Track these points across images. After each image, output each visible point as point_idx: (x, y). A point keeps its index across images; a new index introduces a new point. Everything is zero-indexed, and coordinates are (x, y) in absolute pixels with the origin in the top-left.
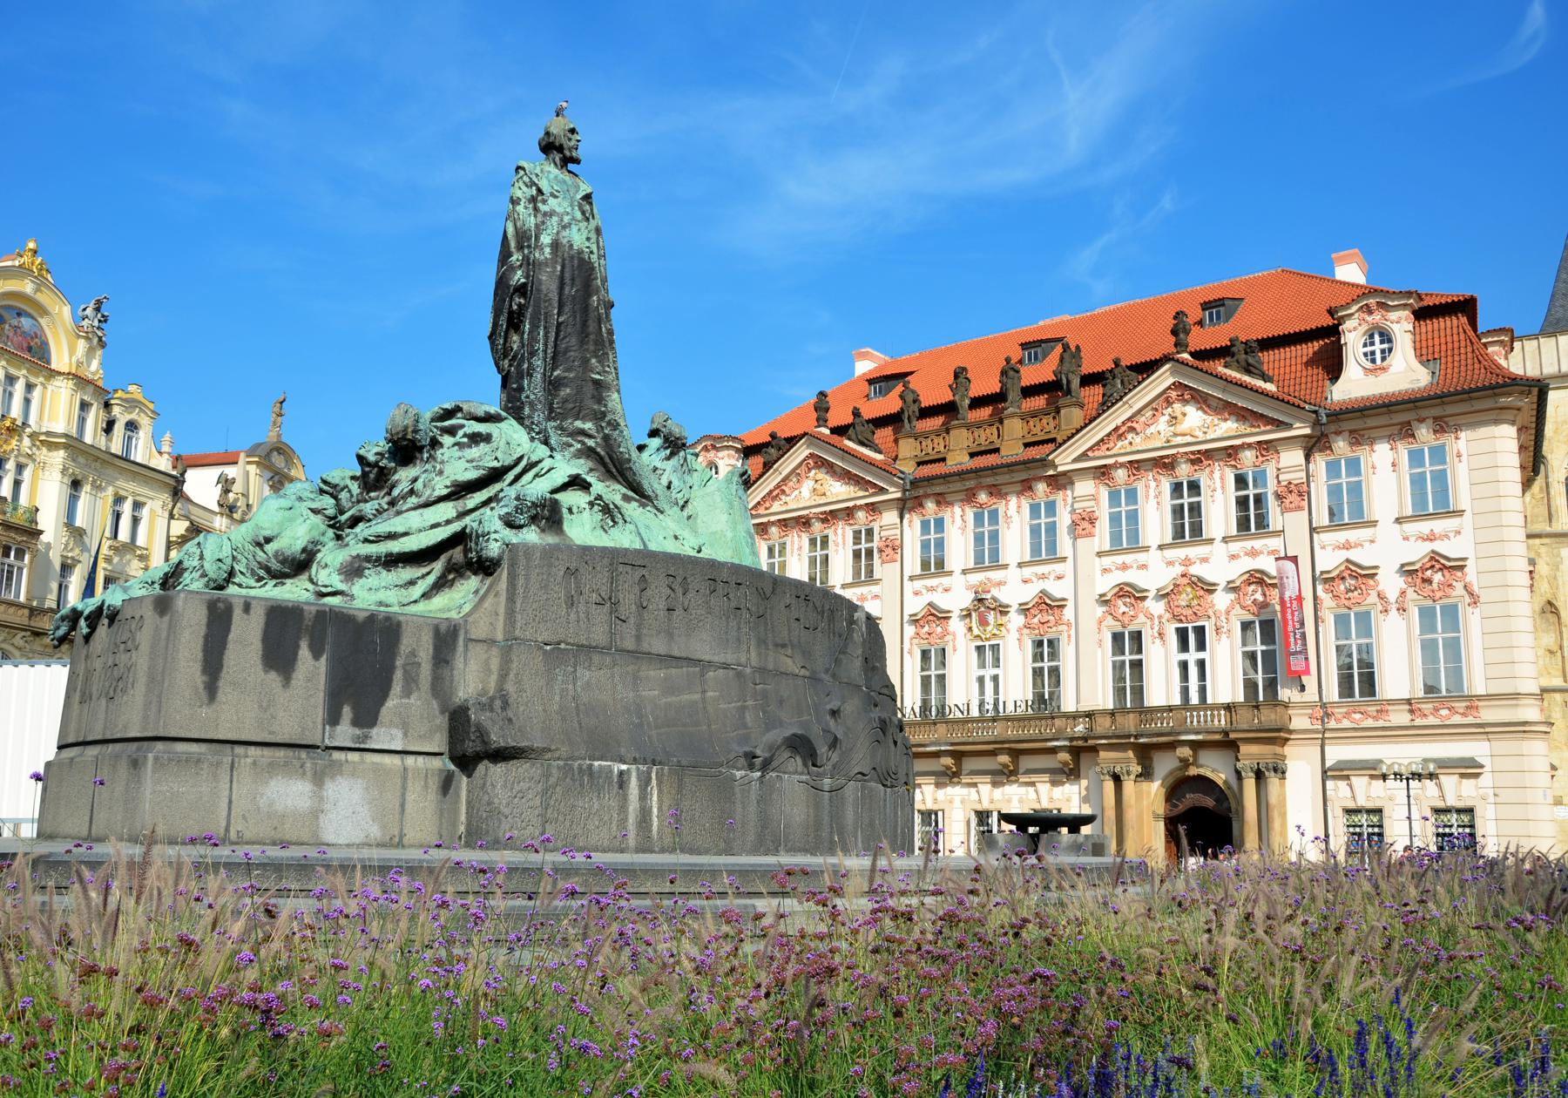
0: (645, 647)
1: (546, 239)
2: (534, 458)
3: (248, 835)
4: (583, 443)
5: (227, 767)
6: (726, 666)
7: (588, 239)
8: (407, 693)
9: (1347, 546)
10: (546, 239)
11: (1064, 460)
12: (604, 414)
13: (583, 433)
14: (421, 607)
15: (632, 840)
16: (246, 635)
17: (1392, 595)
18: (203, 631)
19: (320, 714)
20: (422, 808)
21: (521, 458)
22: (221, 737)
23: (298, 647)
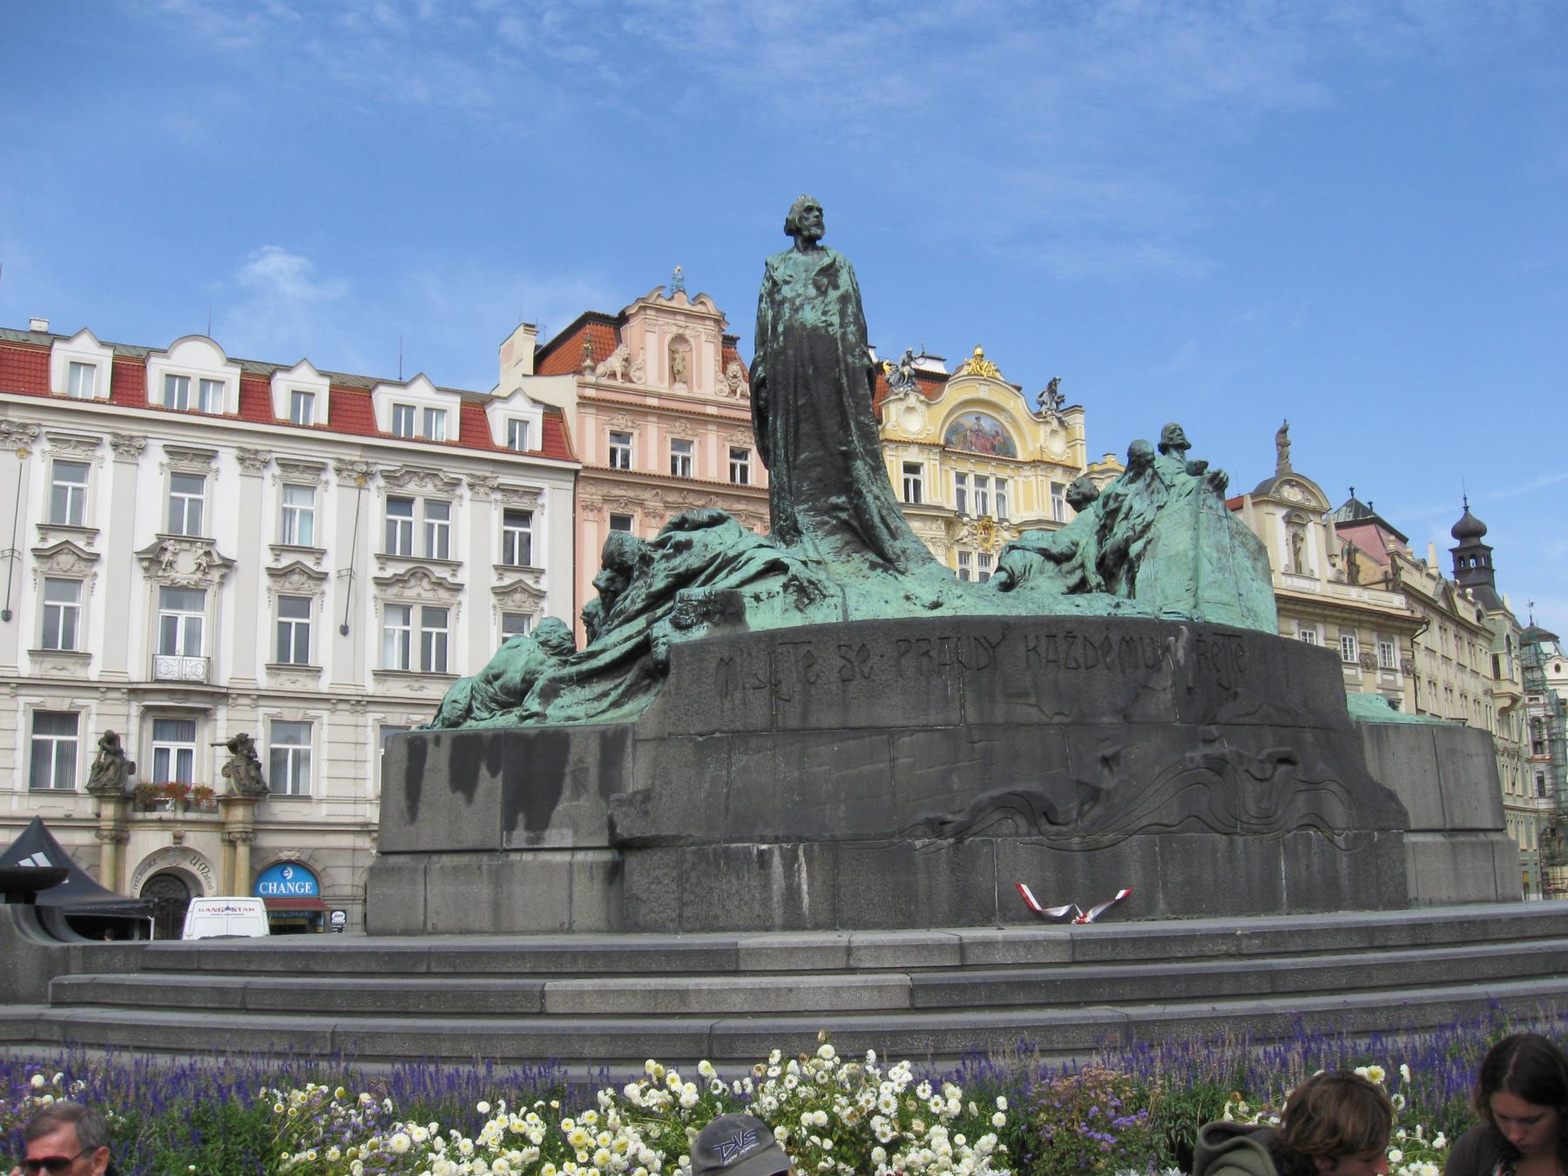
0: (812, 722)
1: (780, 329)
2: (731, 553)
3: (441, 926)
4: (837, 518)
5: (421, 872)
6: (927, 729)
7: (825, 313)
8: (576, 795)
10: (780, 329)
12: (851, 484)
13: (837, 508)
14: (609, 715)
15: (778, 919)
18: (404, 764)
19: (498, 822)
20: (589, 898)
21: (717, 556)
22: (421, 848)
23: (477, 769)
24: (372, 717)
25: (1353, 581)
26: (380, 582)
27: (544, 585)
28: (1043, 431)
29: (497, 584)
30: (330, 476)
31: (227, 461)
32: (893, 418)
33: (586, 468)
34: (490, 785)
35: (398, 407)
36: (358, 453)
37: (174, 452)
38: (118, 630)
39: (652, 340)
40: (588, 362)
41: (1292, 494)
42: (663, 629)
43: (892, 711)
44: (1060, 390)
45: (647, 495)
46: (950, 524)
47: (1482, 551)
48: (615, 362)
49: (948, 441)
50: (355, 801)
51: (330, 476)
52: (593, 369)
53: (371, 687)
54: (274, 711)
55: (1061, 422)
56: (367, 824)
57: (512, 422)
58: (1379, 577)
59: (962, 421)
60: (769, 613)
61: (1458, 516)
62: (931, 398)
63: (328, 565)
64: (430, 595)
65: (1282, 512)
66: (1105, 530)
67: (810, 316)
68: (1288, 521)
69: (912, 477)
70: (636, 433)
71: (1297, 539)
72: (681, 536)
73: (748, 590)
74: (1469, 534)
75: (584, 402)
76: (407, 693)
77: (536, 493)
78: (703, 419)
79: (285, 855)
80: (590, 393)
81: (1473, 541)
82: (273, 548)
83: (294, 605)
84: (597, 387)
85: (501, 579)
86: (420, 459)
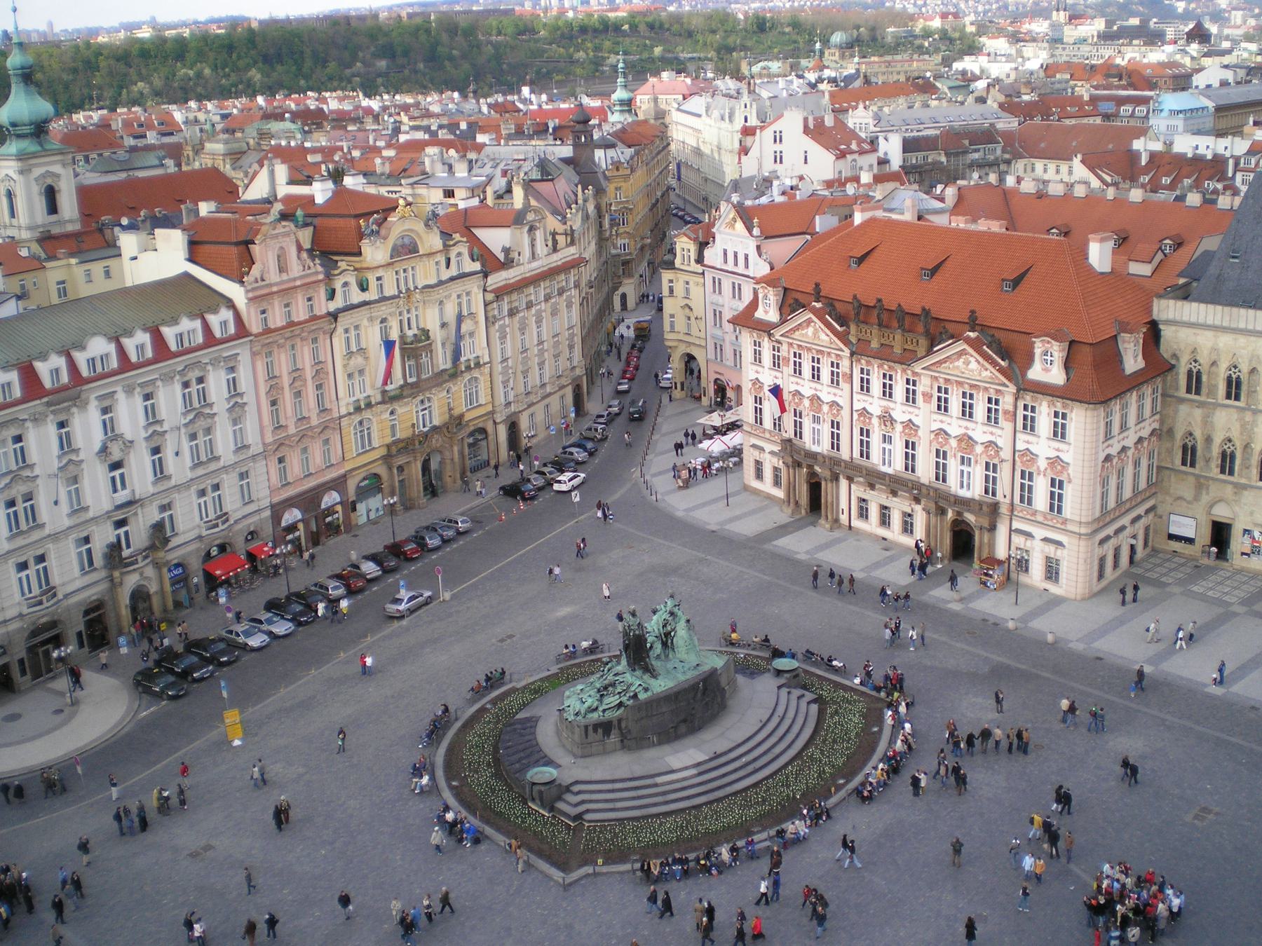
9: (1028, 442)
11: (918, 367)
17: (1042, 469)
24: (193, 489)
30: (159, 383)
31: (121, 396)
34: (600, 731)
37: (101, 398)
38: (98, 493)
43: (664, 710)
48: (256, 271)
50: (193, 529)
51: (159, 383)
75: (251, 300)
80: (251, 295)
83: (156, 451)
84: (253, 289)
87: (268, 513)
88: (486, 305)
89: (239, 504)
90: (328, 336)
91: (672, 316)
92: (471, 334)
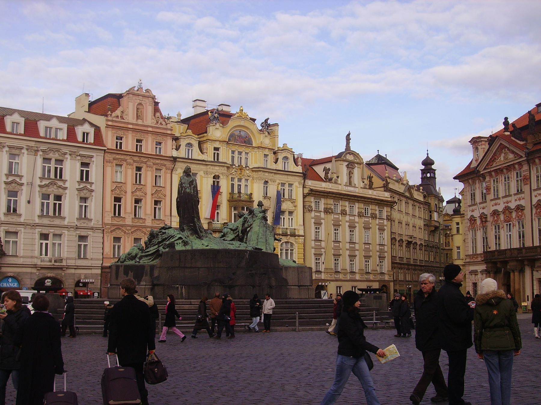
8: (146, 276)
16: (121, 270)
25: (371, 188)
26: (40, 186)
27: (93, 187)
28: (262, 136)
29: (78, 187)
30: (24, 151)
32: (211, 132)
33: (108, 149)
35: (46, 127)
36: (34, 143)
39: (131, 105)
40: (109, 113)
41: (350, 158)
42: (161, 248)
44: (269, 122)
45: (128, 157)
46: (228, 168)
47: (432, 171)
48: (118, 112)
49: (229, 140)
50: (32, 257)
51: (24, 151)
52: (111, 115)
53: (37, 220)
54: (6, 228)
55: (269, 133)
56: (36, 265)
57: (84, 133)
58: (382, 185)
59: (234, 132)
60: (179, 247)
61: (425, 157)
62: (224, 124)
63: (24, 181)
64: (57, 190)
65: (347, 163)
66: (243, 224)
67: (188, 190)
68: (348, 166)
69: (216, 152)
70: (125, 137)
71: (350, 175)
72: (164, 231)
73: (176, 242)
74: (428, 163)
75: (108, 126)
76: (48, 223)
77: (92, 157)
78: (148, 132)
79: (9, 274)
80: (110, 123)
81: (429, 166)
82: (6, 175)
84: (112, 121)
85: (79, 185)
86: (54, 145)
87: (99, 271)
88: (304, 197)
89: (75, 255)
90: (169, 171)
91: (458, 248)
92: (291, 213)
